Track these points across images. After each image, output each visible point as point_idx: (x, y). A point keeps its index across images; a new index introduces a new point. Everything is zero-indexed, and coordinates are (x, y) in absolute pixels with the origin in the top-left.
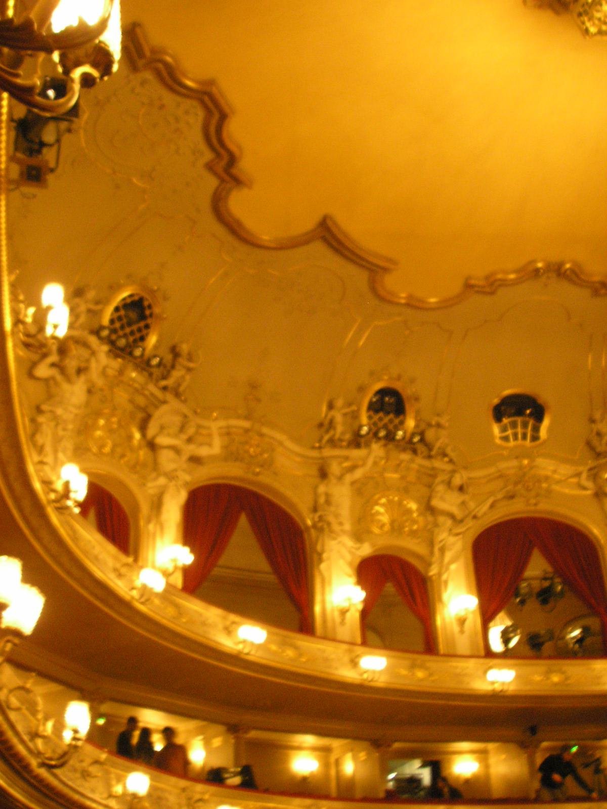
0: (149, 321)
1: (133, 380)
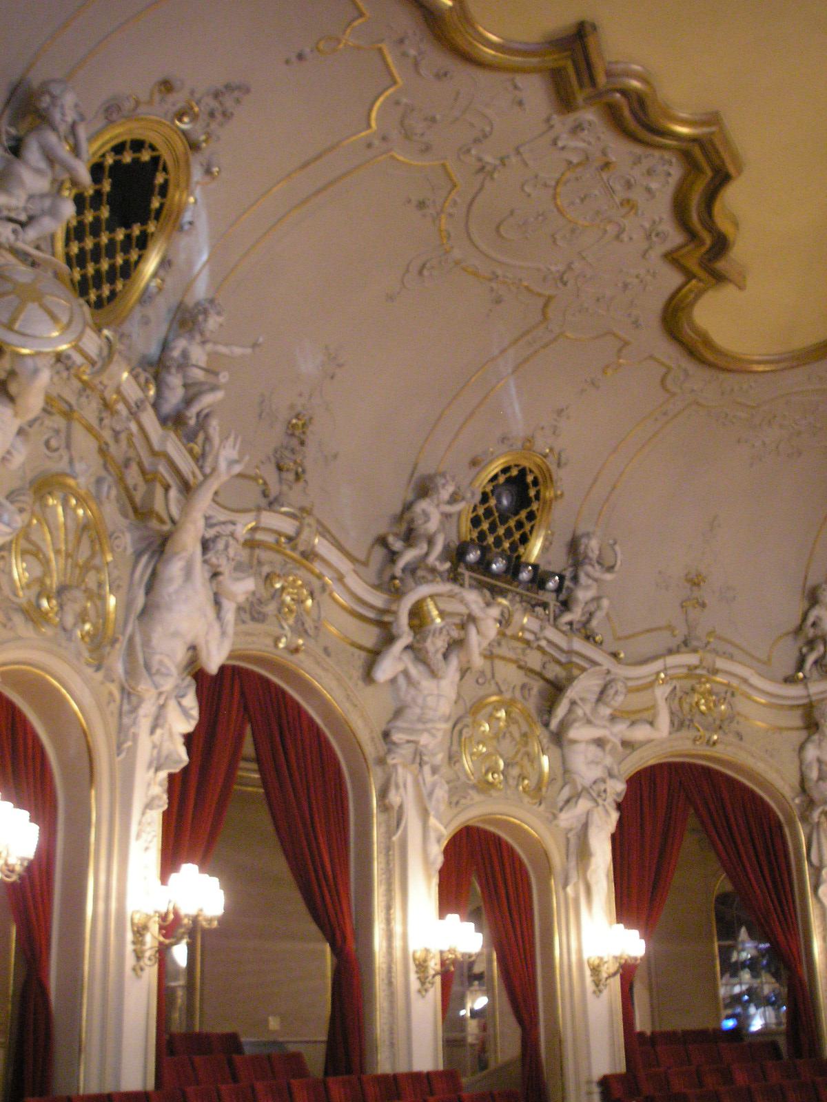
0: (535, 506)
1: (523, 629)
